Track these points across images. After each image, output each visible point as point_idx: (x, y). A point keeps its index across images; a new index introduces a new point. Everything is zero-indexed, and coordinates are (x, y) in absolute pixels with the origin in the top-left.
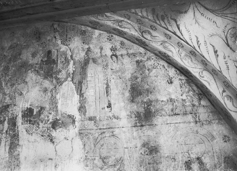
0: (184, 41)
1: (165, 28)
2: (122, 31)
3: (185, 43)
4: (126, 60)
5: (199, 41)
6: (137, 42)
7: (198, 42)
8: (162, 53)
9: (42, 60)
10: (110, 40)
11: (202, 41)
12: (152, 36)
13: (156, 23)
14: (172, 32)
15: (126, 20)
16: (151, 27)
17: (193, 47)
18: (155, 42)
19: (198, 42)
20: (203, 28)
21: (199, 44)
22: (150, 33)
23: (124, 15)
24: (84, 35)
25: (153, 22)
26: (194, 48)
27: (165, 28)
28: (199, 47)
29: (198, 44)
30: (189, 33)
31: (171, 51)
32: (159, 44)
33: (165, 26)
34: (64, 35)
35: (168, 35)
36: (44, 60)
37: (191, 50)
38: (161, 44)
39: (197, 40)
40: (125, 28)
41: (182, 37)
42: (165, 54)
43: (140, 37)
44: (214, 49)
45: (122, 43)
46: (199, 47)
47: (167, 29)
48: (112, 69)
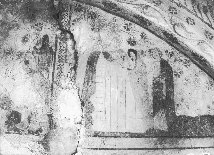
1: (208, 24)
2: (148, 20)
4: (148, 60)
6: (164, 37)
9: (35, 48)
10: (128, 29)
12: (186, 31)
13: (197, 16)
15: (153, 5)
16: (187, 19)
18: (190, 41)
22: (183, 27)
24: (94, 19)
25: (193, 14)
27: (208, 24)
31: (210, 55)
32: (196, 43)
33: (208, 22)
34: (66, 16)
36: (38, 47)
38: (198, 44)
40: (151, 16)
42: (202, 57)
43: (171, 32)
45: (143, 37)
48: (129, 70)
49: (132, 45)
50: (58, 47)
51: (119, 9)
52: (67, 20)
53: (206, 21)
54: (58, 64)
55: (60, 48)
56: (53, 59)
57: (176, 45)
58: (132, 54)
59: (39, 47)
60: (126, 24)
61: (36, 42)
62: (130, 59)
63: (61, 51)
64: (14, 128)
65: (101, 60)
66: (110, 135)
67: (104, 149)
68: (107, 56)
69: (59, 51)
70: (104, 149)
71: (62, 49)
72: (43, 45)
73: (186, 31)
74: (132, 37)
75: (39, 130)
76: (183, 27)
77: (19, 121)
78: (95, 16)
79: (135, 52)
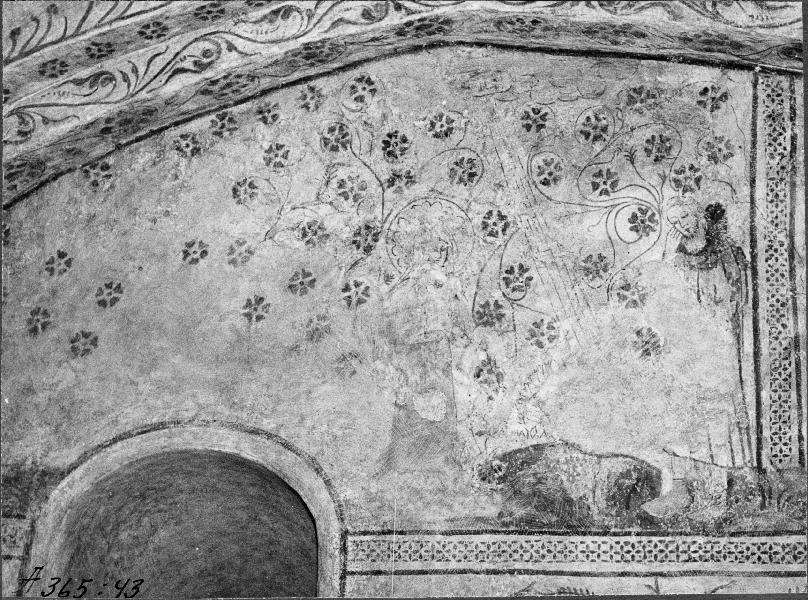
9: (682, 249)
34: (781, 134)
36: (691, 247)
50: (762, 244)
52: (785, 149)
54: (768, 299)
55: (771, 247)
56: (750, 279)
59: (698, 244)
61: (683, 231)
63: (773, 255)
64: (639, 516)
69: (767, 255)
71: (776, 251)
72: (708, 240)
75: (725, 520)
77: (654, 493)
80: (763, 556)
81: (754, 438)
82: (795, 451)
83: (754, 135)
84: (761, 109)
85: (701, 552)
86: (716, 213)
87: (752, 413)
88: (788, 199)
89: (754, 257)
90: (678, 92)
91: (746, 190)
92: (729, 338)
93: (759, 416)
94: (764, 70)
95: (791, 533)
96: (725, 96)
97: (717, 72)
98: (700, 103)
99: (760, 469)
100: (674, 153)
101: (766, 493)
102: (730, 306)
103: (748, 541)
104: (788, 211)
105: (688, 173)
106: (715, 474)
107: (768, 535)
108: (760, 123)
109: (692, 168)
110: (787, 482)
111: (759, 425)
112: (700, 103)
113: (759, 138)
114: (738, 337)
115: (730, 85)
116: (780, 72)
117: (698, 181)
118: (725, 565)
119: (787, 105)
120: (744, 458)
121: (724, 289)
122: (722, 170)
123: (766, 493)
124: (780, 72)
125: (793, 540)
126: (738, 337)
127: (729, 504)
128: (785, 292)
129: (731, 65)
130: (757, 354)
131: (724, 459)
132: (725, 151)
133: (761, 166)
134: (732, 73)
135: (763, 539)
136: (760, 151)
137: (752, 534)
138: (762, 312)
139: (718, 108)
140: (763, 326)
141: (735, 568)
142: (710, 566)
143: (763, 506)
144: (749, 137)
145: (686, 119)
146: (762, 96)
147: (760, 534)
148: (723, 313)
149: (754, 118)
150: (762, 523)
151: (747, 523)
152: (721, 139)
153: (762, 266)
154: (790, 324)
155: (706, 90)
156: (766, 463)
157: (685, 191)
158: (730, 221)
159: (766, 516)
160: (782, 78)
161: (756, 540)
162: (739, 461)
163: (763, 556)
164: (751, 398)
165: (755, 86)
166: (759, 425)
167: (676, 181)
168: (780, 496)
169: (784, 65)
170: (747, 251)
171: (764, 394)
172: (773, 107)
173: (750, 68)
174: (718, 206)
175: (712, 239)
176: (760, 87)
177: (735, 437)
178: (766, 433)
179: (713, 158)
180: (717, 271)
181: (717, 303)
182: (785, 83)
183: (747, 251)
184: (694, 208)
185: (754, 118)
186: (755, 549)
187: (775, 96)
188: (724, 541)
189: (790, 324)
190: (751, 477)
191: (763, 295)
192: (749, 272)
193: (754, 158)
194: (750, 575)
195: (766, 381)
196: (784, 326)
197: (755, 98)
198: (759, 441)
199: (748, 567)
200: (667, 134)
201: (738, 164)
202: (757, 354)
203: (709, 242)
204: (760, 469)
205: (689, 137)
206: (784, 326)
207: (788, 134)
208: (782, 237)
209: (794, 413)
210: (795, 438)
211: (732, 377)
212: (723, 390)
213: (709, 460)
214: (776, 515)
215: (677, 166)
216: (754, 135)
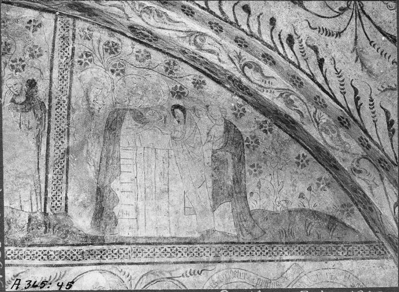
0: (327, 93)
1: (293, 63)
3: (331, 101)
5: (358, 98)
7: (357, 99)
8: (281, 114)
9: (13, 101)
10: (171, 72)
11: (365, 101)
12: (263, 75)
14: (308, 75)
17: (346, 110)
18: (269, 90)
19: (357, 99)
20: (370, 72)
21: (359, 104)
22: (258, 69)
23: (210, 23)
24: (114, 53)
25: (271, 48)
26: (349, 112)
27: (293, 63)
28: (358, 111)
29: (356, 103)
30: (341, 79)
32: (277, 94)
33: (293, 59)
34: (67, 47)
35: (298, 78)
36: (17, 100)
37: (340, 114)
39: (355, 96)
41: (326, 87)
44: (388, 117)
45: (198, 84)
46: (358, 111)
47: (299, 67)
48: (173, 138)
49: (179, 97)
50: (54, 101)
51: (157, 38)
52: (69, 54)
53: (289, 57)
54: (55, 128)
55: (59, 103)
56: (47, 118)
57: (249, 98)
58: (178, 112)
60: (169, 64)
61: (14, 91)
62: (175, 121)
63: (59, 107)
65: (129, 122)
66: (144, 241)
67: (137, 264)
68: (139, 117)
69: (57, 107)
70: (137, 264)
71: (61, 105)
72: (27, 97)
73: (263, 75)
74: (179, 86)
75: (26, 239)
76: (258, 69)
78: (116, 49)
79: (183, 110)
80: (44, 257)
81: (43, 197)
82: (63, 204)
83: (54, 46)
84: (58, 33)
85: (12, 255)
86: (32, 84)
87: (43, 185)
88: (69, 80)
89: (50, 107)
90: (17, 21)
91: (47, 73)
92: (33, 147)
93: (46, 187)
94: (61, 14)
95: (58, 245)
96: (40, 25)
97: (37, 13)
98: (27, 27)
99: (45, 213)
100: (12, 52)
101: (47, 225)
102: (36, 131)
103: (37, 249)
104: (68, 85)
105: (18, 62)
106: (22, 216)
107: (47, 246)
108: (57, 41)
109: (20, 60)
110: (59, 221)
111: (46, 191)
112: (27, 27)
113: (56, 47)
114: (39, 147)
115: (43, 20)
116: (68, 16)
117: (23, 67)
118: (25, 261)
119: (71, 32)
120: (38, 207)
121: (33, 122)
122: (36, 62)
123: (47, 225)
124: (68, 16)
125: (60, 248)
126: (39, 147)
127: (28, 230)
128: (64, 126)
129: (44, 10)
130: (47, 156)
131: (27, 208)
132: (38, 53)
133: (56, 62)
134: (45, 14)
135: (45, 248)
136: (56, 55)
137: (39, 246)
138: (52, 135)
139: (36, 31)
140: (52, 142)
141: (30, 262)
142: (17, 262)
143: (45, 232)
144: (51, 47)
145: (19, 35)
146: (59, 27)
147: (43, 246)
148: (32, 134)
149: (54, 37)
150: (45, 240)
151: (37, 240)
152: (37, 46)
153: (53, 112)
154: (66, 141)
155: (30, 21)
156: (48, 210)
157: (16, 71)
158: (39, 88)
159: (47, 237)
160: (70, 19)
161: (41, 249)
162: (35, 209)
163: (44, 257)
164: (43, 178)
165: (56, 20)
166: (46, 191)
167: (12, 66)
168: (54, 227)
169: (71, 13)
170: (47, 104)
171: (50, 176)
172: (64, 33)
173: (54, 12)
174: (33, 80)
175: (29, 97)
176: (58, 22)
177: (34, 197)
178: (50, 195)
179: (32, 56)
180: (31, 113)
181: (29, 129)
182: (71, 21)
183: (47, 104)
184: (21, 80)
185: (54, 37)
186: (40, 253)
187: (65, 27)
188: (24, 249)
189: (66, 141)
190: (40, 217)
191: (53, 126)
192: (47, 114)
193: (52, 57)
194: (37, 266)
195: (51, 170)
196: (62, 142)
197: (55, 27)
198: (46, 199)
199: (36, 262)
200: (9, 41)
201: (45, 60)
202: (47, 156)
203: (27, 98)
204: (45, 213)
205: (20, 44)
206: (62, 142)
207: (71, 47)
208: (65, 98)
209: (64, 186)
210: (64, 198)
211: (33, 167)
212: (28, 173)
213: (19, 209)
214: (52, 236)
215: (13, 58)
216: (54, 46)
